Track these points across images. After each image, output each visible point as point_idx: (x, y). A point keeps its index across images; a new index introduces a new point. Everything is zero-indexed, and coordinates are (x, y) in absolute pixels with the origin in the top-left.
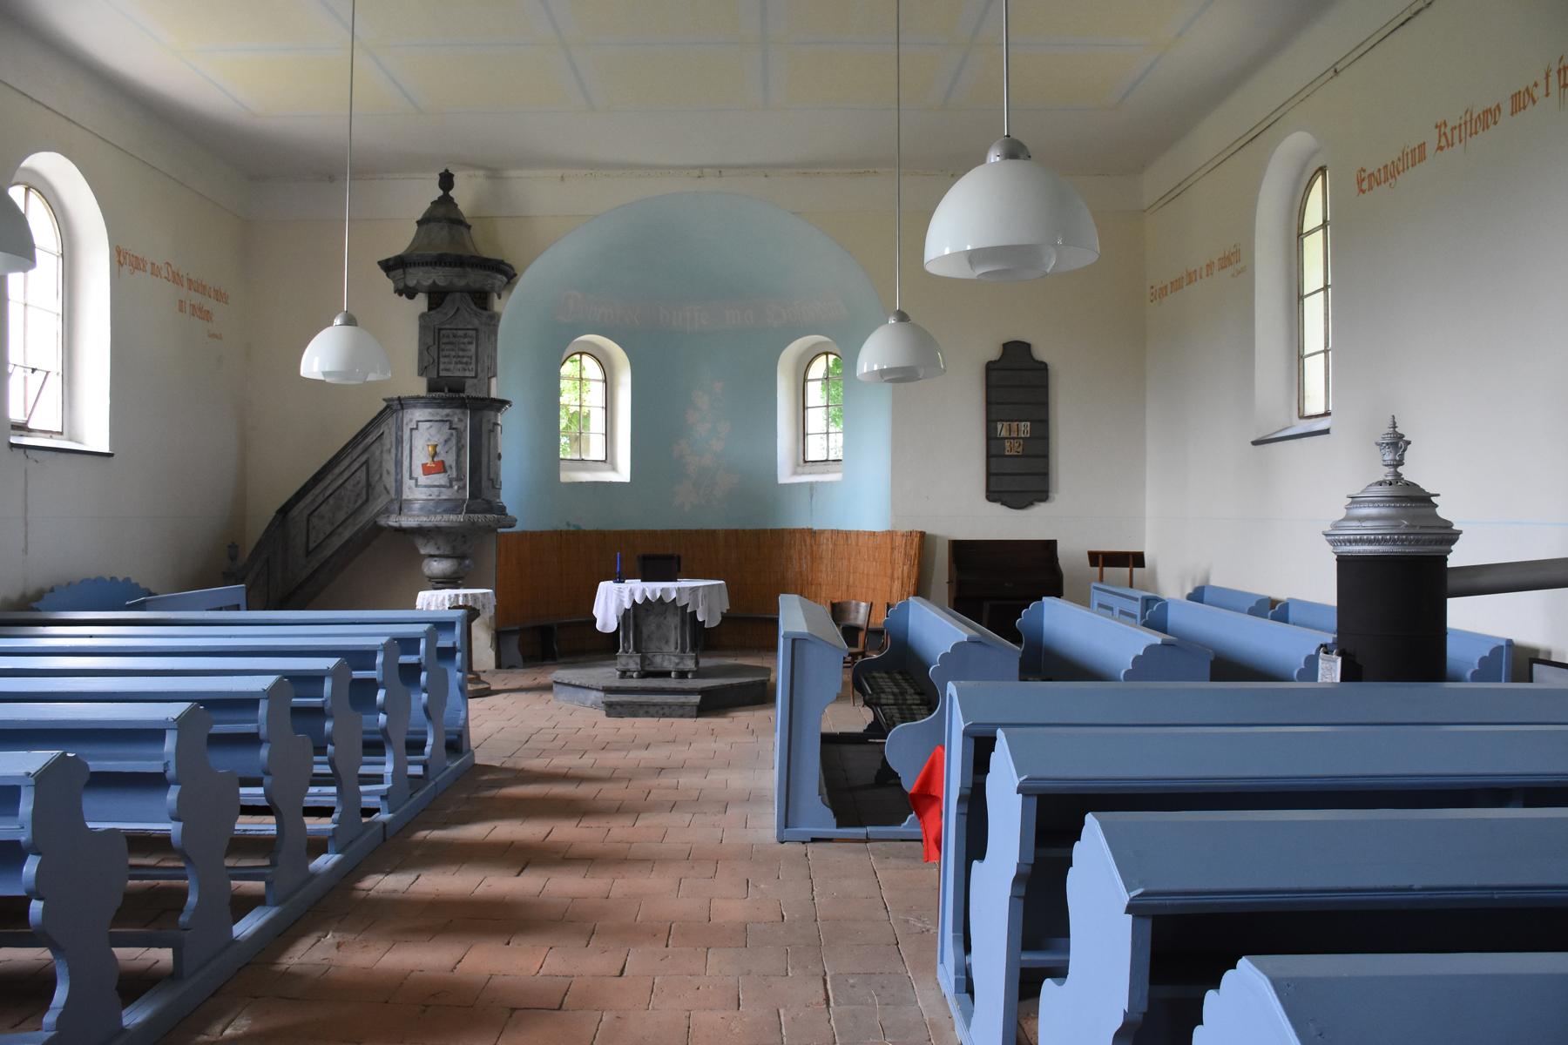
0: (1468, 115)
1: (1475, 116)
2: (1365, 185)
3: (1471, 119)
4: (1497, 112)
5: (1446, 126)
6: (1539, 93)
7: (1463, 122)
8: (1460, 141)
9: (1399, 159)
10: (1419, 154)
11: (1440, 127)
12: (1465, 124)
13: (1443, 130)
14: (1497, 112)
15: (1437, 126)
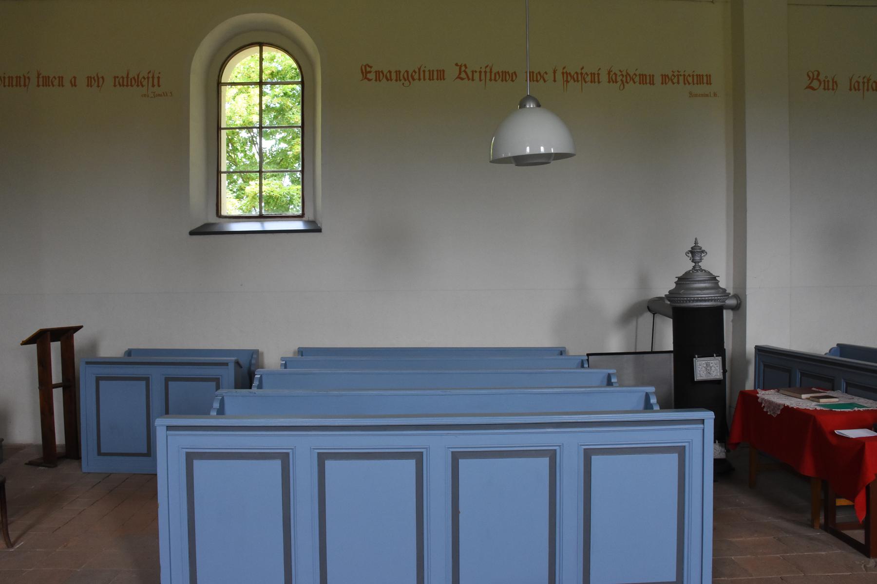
0: (488, 70)
1: (494, 71)
2: (371, 76)
3: (491, 72)
4: (514, 76)
5: (466, 67)
6: (549, 77)
7: (483, 70)
8: (481, 80)
9: (414, 71)
10: (441, 75)
11: (461, 66)
12: (485, 72)
13: (463, 68)
14: (514, 76)
15: (457, 65)
